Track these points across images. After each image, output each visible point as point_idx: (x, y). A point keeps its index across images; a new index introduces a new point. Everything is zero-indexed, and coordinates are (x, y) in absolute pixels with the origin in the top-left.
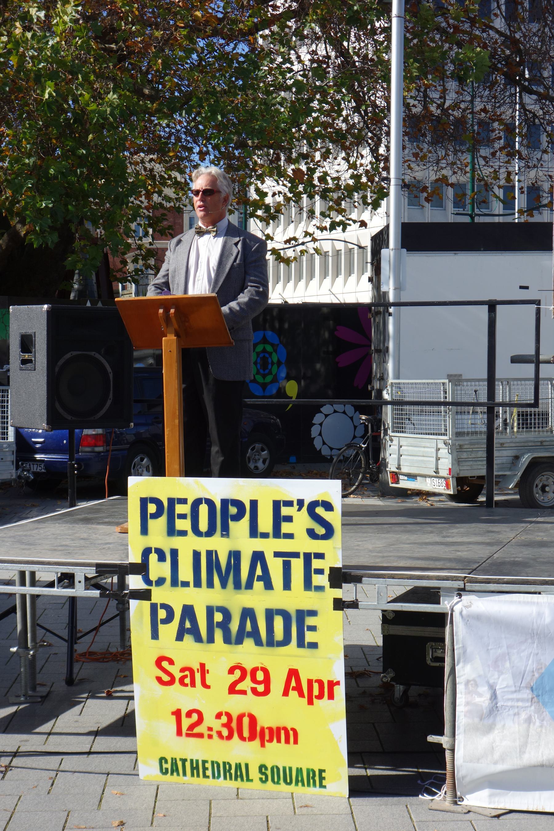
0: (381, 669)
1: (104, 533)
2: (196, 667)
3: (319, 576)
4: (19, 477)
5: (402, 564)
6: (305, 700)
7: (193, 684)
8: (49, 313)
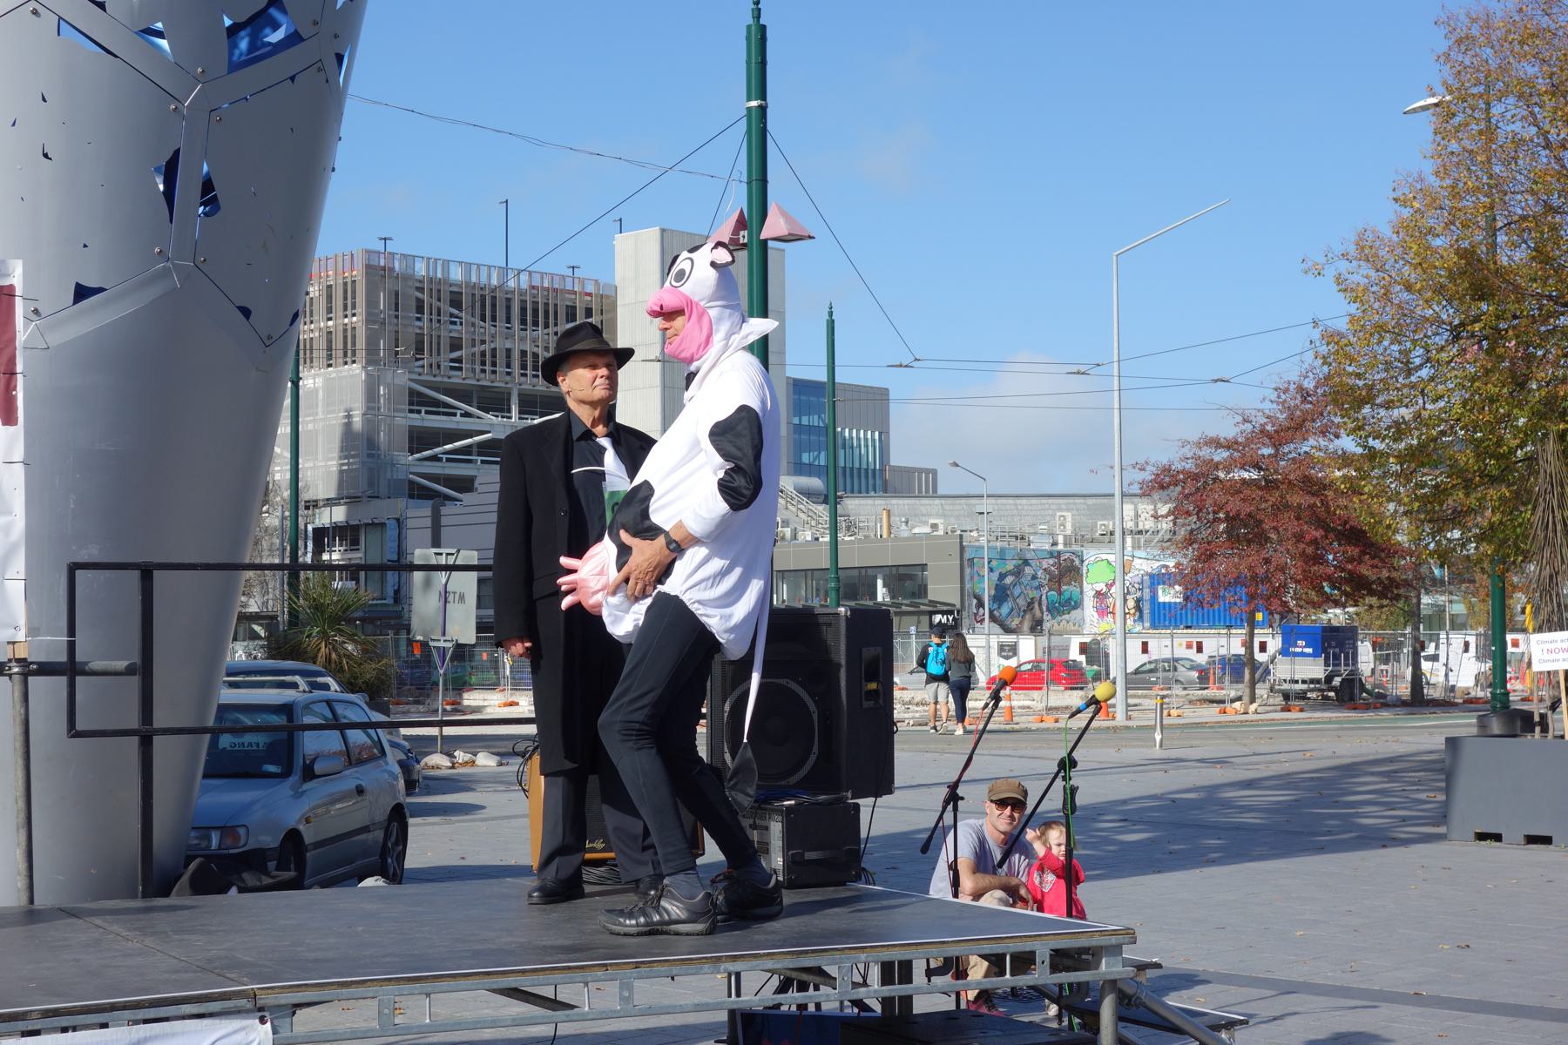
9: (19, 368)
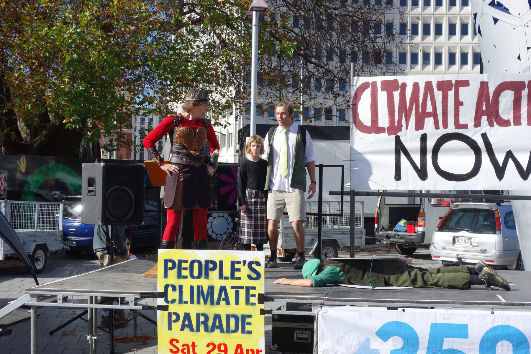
0: (271, 344)
1: (139, 277)
2: (190, 344)
3: (253, 298)
4: (63, 248)
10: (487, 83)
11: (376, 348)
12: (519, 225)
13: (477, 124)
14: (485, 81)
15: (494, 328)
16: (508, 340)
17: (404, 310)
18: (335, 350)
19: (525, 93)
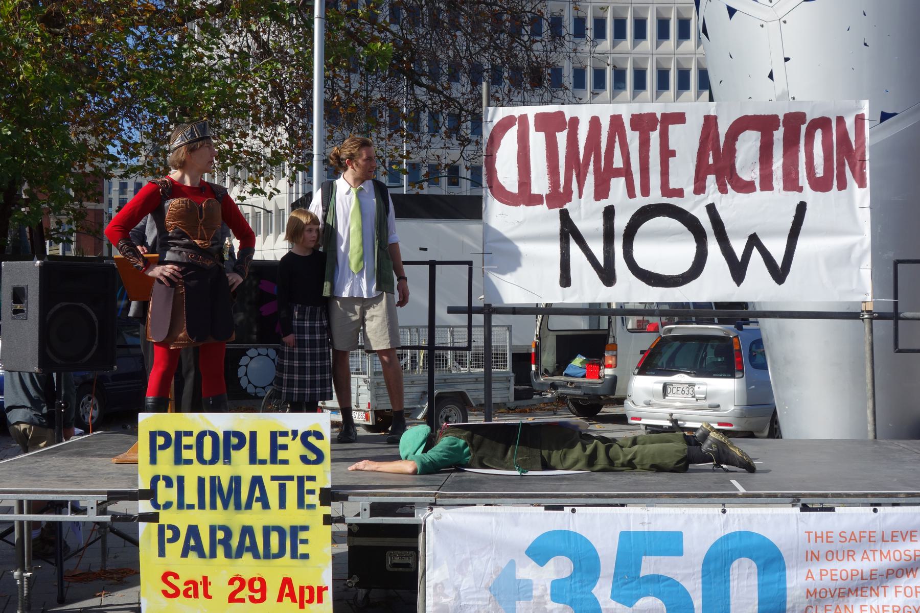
0: (346, 576)
1: (107, 465)
2: (199, 579)
5: (378, 483)
6: (298, 604)
7: (196, 595)
8: (41, 267)
9: (867, 157)
10: (715, 118)
11: (526, 577)
12: (773, 362)
13: (700, 188)
14: (712, 114)
15: (727, 538)
16: (751, 558)
17: (573, 511)
18: (456, 584)
19: (778, 135)
